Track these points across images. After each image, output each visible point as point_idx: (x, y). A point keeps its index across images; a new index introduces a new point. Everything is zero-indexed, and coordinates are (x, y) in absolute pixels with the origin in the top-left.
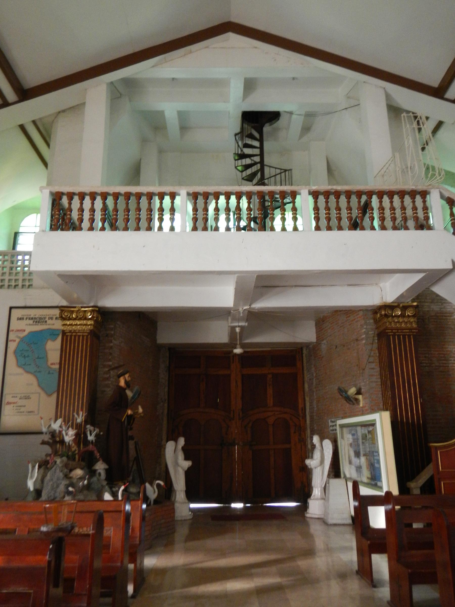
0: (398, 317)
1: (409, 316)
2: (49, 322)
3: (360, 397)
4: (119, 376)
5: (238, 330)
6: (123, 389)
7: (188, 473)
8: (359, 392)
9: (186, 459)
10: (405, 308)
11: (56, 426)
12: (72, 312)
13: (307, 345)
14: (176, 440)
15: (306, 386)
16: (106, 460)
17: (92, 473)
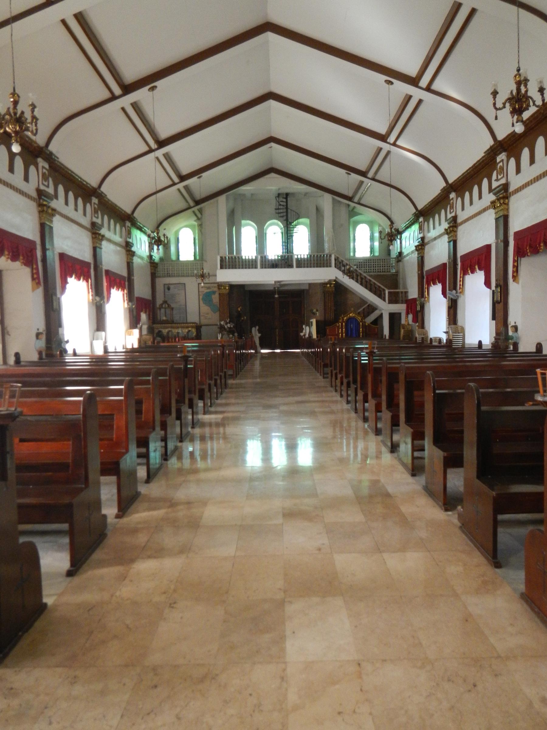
0: (328, 287)
1: (332, 287)
2: (212, 288)
3: (317, 312)
4: (238, 307)
5: (276, 288)
6: (239, 311)
7: (260, 338)
8: (317, 311)
9: (259, 333)
10: (331, 284)
11: (222, 323)
12: (222, 287)
13: (306, 290)
14: (255, 328)
15: (305, 306)
16: (238, 333)
17: (233, 335)
